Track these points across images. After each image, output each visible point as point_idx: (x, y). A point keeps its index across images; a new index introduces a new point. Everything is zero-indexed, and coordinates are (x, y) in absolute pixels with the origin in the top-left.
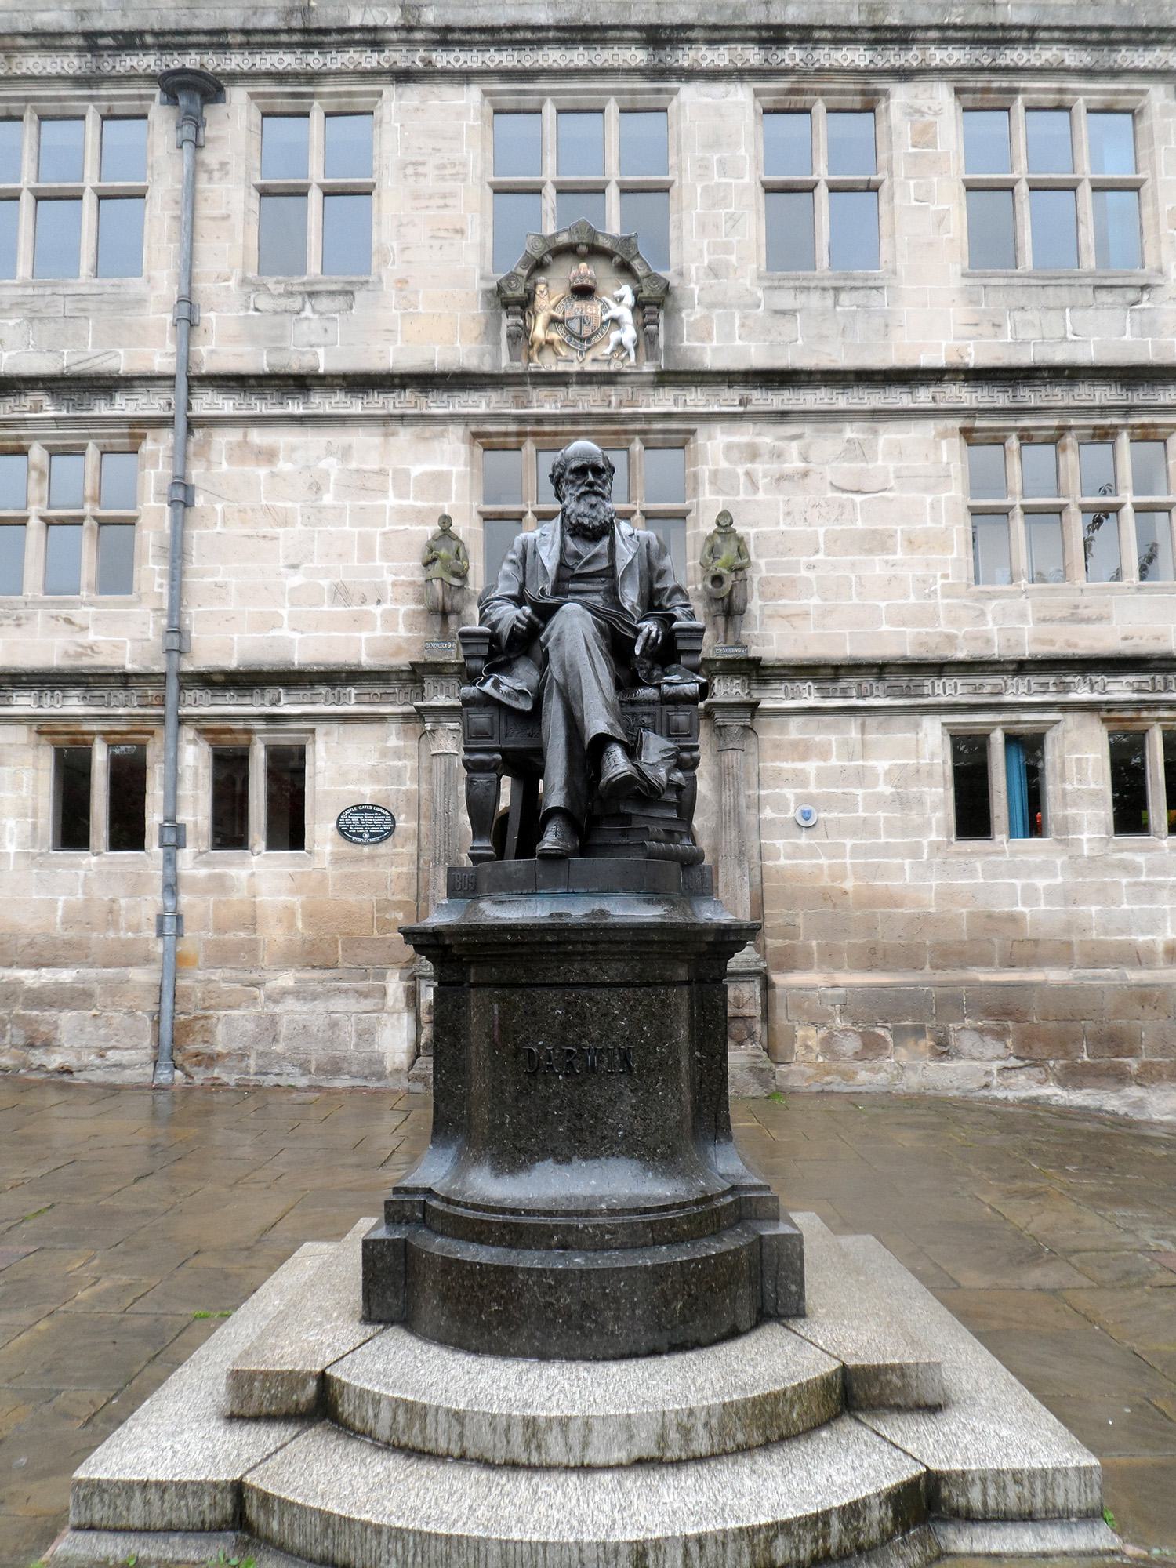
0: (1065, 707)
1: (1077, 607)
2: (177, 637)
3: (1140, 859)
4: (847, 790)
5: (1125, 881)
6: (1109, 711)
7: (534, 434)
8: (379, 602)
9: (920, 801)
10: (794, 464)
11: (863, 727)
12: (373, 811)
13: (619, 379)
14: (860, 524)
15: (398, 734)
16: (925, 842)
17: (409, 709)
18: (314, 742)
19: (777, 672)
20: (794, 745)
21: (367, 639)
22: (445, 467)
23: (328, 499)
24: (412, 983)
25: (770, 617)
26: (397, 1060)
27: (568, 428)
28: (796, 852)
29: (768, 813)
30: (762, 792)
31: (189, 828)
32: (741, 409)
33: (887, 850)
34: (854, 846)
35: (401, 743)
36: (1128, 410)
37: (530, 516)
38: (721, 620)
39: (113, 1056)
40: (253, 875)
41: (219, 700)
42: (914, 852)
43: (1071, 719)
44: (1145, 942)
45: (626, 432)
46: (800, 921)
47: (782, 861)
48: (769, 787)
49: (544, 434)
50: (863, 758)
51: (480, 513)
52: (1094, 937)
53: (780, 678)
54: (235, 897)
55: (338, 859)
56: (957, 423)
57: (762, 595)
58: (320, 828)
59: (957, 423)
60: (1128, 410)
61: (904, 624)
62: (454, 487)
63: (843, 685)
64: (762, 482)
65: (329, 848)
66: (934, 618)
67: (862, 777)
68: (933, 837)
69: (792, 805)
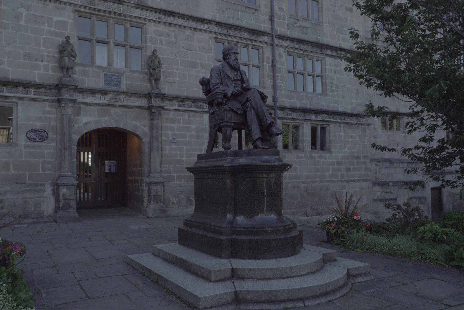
7: (96, 14)
8: (42, 61)
10: (173, 39)
11: (189, 116)
12: (40, 131)
13: (124, 3)
14: (189, 59)
17: (56, 98)
18: (17, 107)
22: (66, 20)
23: (22, 22)
25: (166, 82)
27: (107, 15)
29: (164, 138)
32: (159, 20)
35: (50, 109)
36: (253, 40)
37: (94, 41)
45: (125, 20)
46: (171, 169)
47: (167, 152)
49: (100, 15)
51: (77, 37)
53: (168, 100)
55: (26, 147)
56: (214, 36)
59: (214, 36)
60: (253, 40)
62: (69, 27)
63: (184, 103)
64: (164, 43)
65: (23, 143)
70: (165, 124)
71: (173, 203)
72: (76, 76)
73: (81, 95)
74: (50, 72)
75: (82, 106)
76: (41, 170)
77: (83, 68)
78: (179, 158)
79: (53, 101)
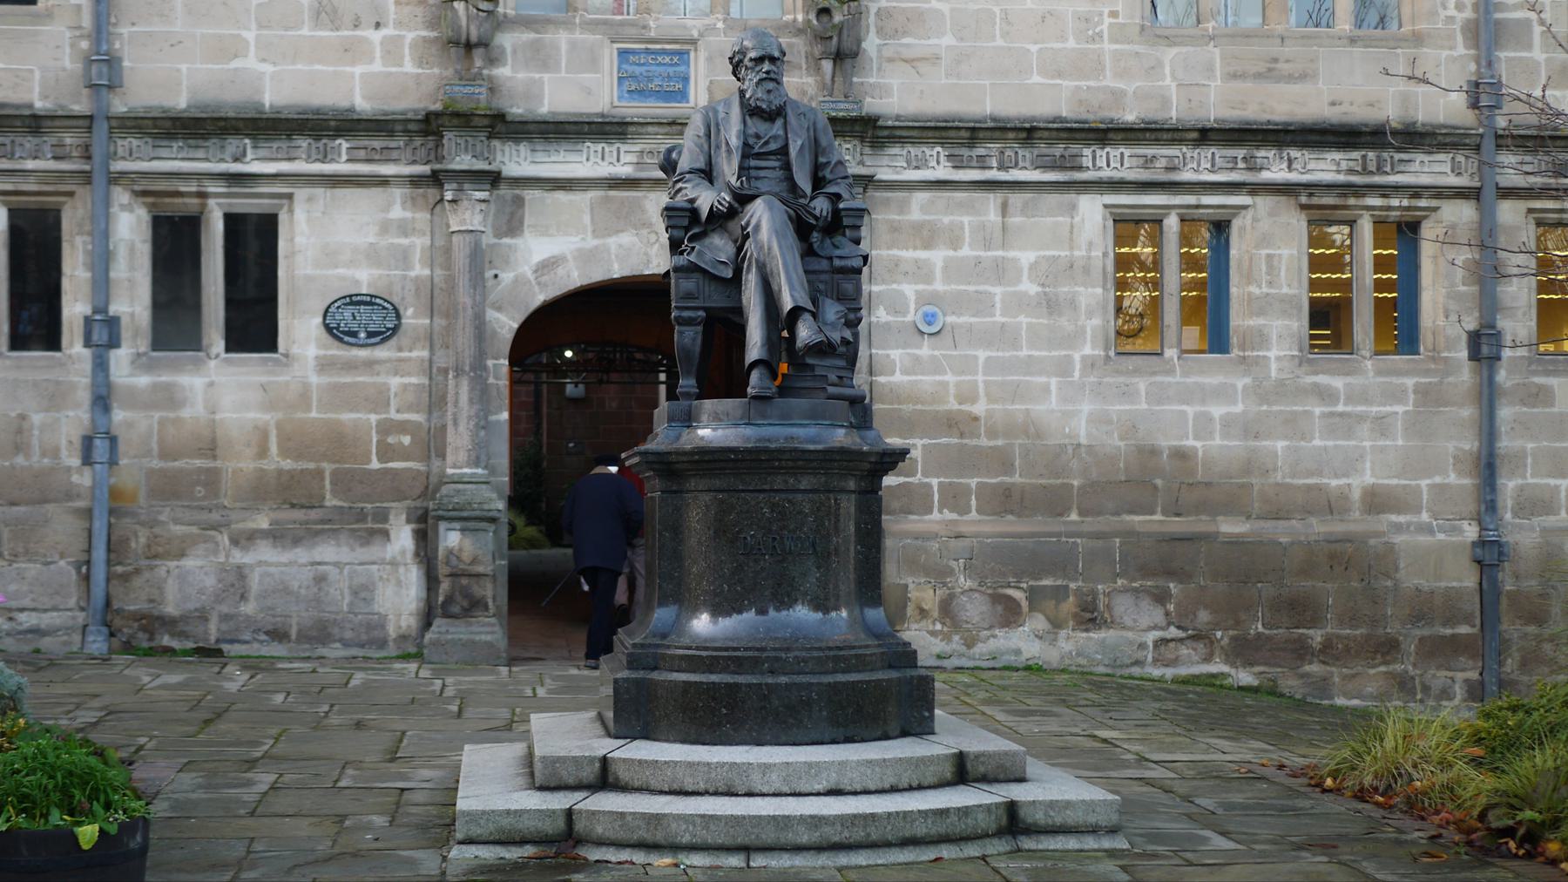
0: (1255, 189)
1: (1276, 60)
2: (103, 68)
3: (1338, 383)
4: (981, 288)
5: (1318, 411)
6: (1311, 195)
8: (378, 25)
9: (1073, 303)
11: (1004, 209)
15: (404, 203)
16: (1077, 357)
17: (425, 169)
18: (291, 211)
19: (898, 133)
20: (918, 227)
21: (362, 75)
24: (422, 526)
25: (890, 60)
26: (404, 624)
28: (916, 366)
30: (875, 288)
31: (124, 321)
33: (1030, 365)
34: (988, 359)
35: (408, 215)
38: (827, 65)
39: (27, 620)
40: (211, 384)
41: (164, 153)
42: (1063, 368)
43: (1263, 203)
44: (1339, 487)
47: (898, 378)
48: (884, 282)
50: (1003, 247)
52: (1279, 479)
54: (186, 413)
55: (324, 365)
57: (880, 31)
58: (300, 328)
61: (1060, 75)
63: (981, 151)
65: (312, 351)
66: (1098, 69)
67: (1001, 271)
68: (1088, 350)
69: (912, 307)
70: (884, 253)
71: (923, 614)
72: (503, 72)
73: (523, 148)
74: (409, 67)
75: (530, 195)
76: (374, 458)
77: (533, 35)
78: (953, 405)
79: (415, 181)
